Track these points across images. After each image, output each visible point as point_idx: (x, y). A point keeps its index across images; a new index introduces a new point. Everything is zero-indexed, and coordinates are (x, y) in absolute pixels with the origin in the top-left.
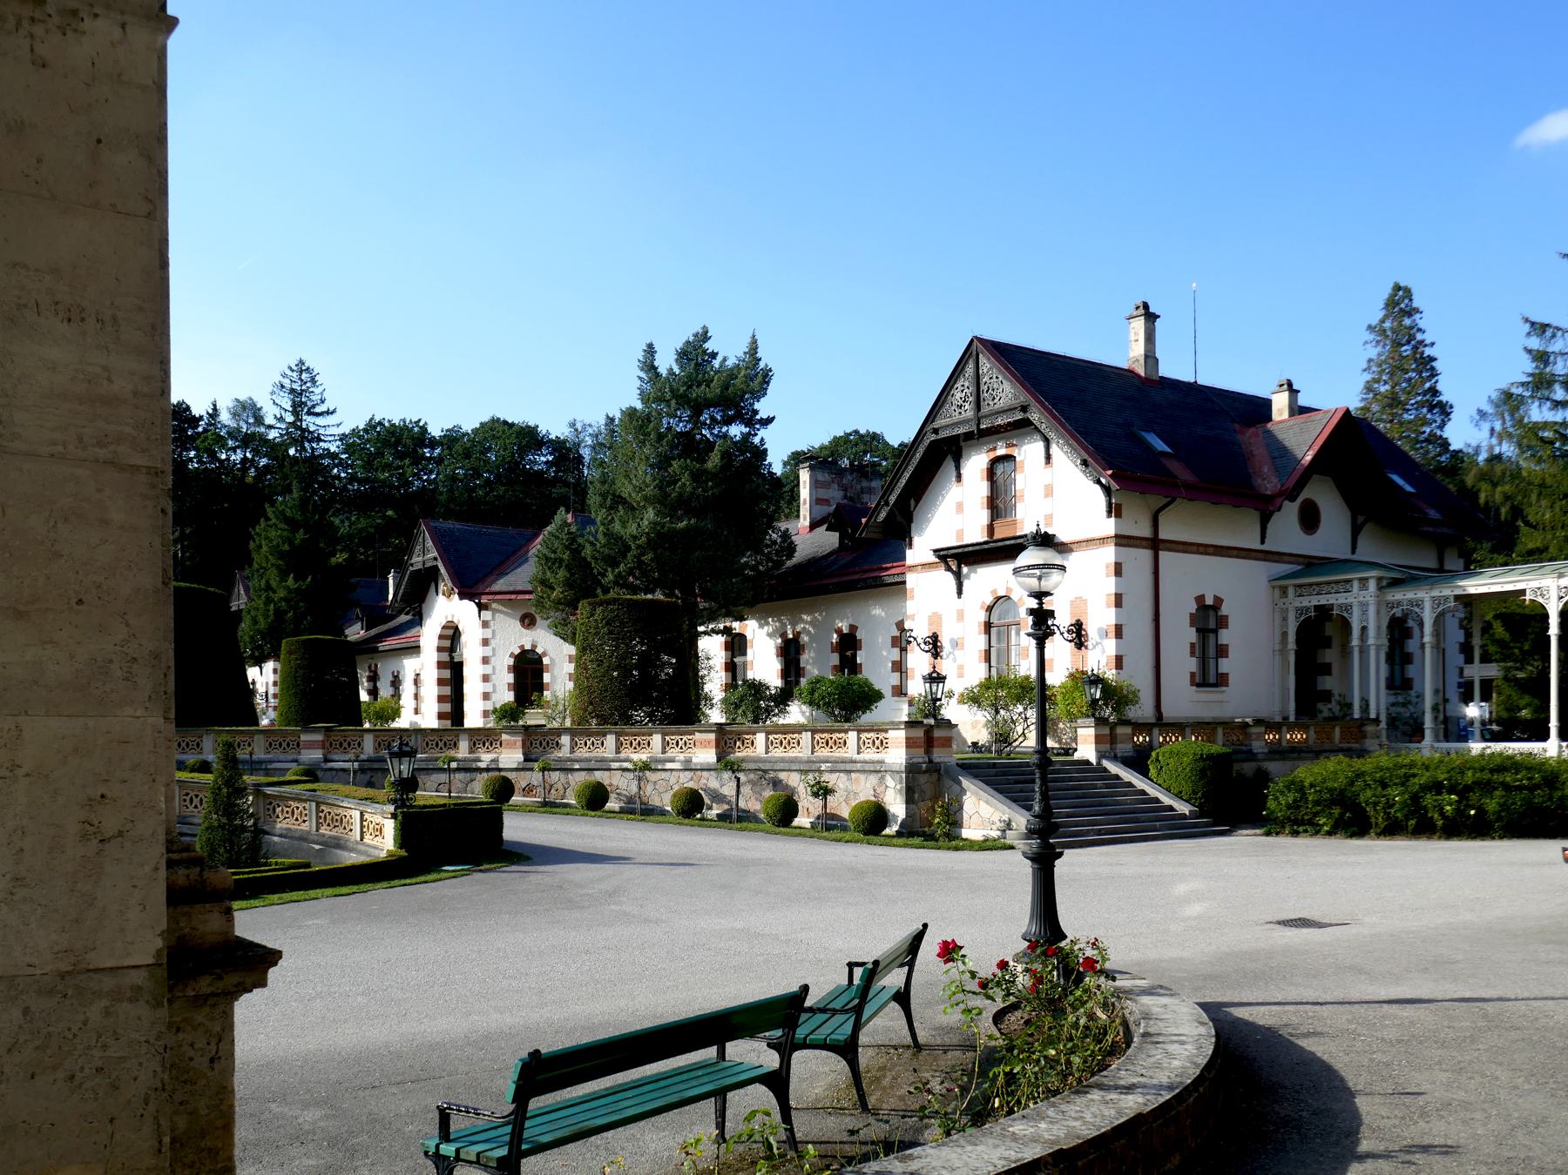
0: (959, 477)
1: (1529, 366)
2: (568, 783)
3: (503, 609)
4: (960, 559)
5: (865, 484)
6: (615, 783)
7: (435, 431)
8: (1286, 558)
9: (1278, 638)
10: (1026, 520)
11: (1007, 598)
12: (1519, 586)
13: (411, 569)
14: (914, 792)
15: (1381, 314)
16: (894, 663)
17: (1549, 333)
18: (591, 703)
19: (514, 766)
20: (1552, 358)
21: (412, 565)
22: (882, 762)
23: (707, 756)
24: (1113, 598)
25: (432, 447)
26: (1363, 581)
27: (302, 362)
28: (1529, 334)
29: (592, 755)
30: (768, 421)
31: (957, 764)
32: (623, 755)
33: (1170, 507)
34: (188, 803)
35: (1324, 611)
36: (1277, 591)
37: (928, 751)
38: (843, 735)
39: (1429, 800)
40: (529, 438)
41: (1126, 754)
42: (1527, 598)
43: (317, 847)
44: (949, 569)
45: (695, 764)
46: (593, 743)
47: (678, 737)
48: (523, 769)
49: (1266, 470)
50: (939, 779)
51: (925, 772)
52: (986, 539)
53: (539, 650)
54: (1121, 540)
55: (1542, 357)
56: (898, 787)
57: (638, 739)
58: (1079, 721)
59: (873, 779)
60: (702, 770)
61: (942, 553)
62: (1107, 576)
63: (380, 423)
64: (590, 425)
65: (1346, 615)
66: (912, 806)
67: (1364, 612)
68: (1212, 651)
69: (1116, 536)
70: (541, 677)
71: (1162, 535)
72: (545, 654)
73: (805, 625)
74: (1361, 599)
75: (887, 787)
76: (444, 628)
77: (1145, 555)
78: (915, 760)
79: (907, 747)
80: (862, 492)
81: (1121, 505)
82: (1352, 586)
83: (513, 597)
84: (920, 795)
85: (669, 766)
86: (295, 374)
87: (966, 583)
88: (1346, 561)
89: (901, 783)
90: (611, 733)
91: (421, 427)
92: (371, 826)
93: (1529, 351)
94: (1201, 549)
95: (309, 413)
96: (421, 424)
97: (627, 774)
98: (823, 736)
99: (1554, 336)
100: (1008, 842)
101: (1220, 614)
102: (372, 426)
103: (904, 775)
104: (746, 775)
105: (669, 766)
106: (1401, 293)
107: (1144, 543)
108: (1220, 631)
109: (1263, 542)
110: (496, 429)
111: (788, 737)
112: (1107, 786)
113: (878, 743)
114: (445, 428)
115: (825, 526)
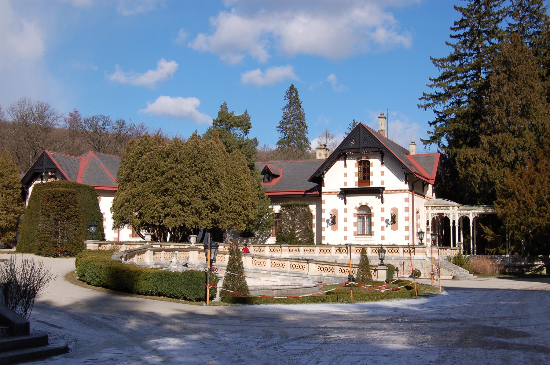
4: (345, 193)
10: (375, 182)
38: (397, 249)
62: (405, 202)
65: (448, 216)
67: (454, 216)
74: (453, 212)
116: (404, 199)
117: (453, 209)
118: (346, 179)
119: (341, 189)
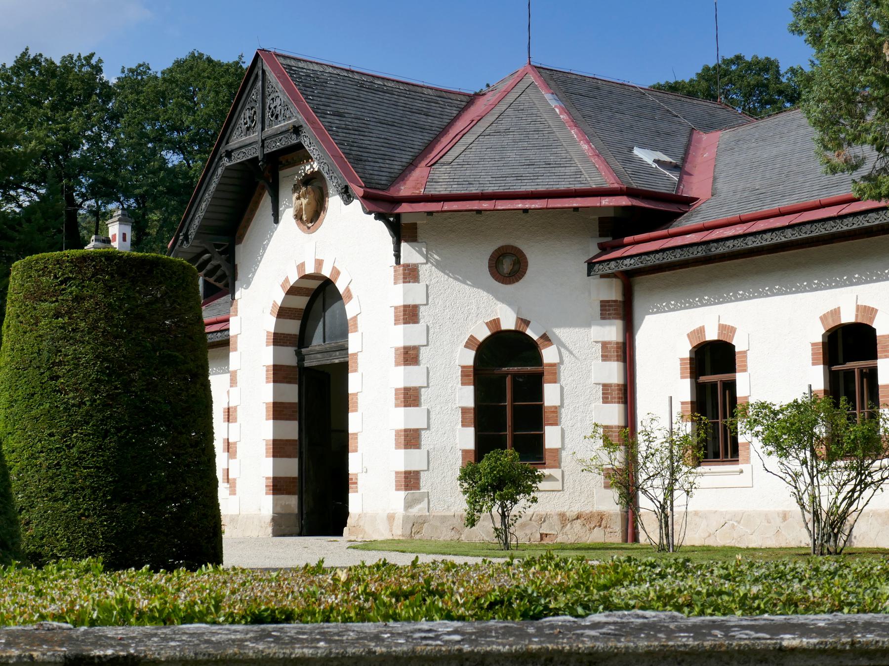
7: (111, 76)
13: (226, 162)
63: (36, 61)
76: (293, 291)
83: (485, 205)
91: (92, 67)
96: (93, 61)
102: (25, 64)
114: (127, 67)
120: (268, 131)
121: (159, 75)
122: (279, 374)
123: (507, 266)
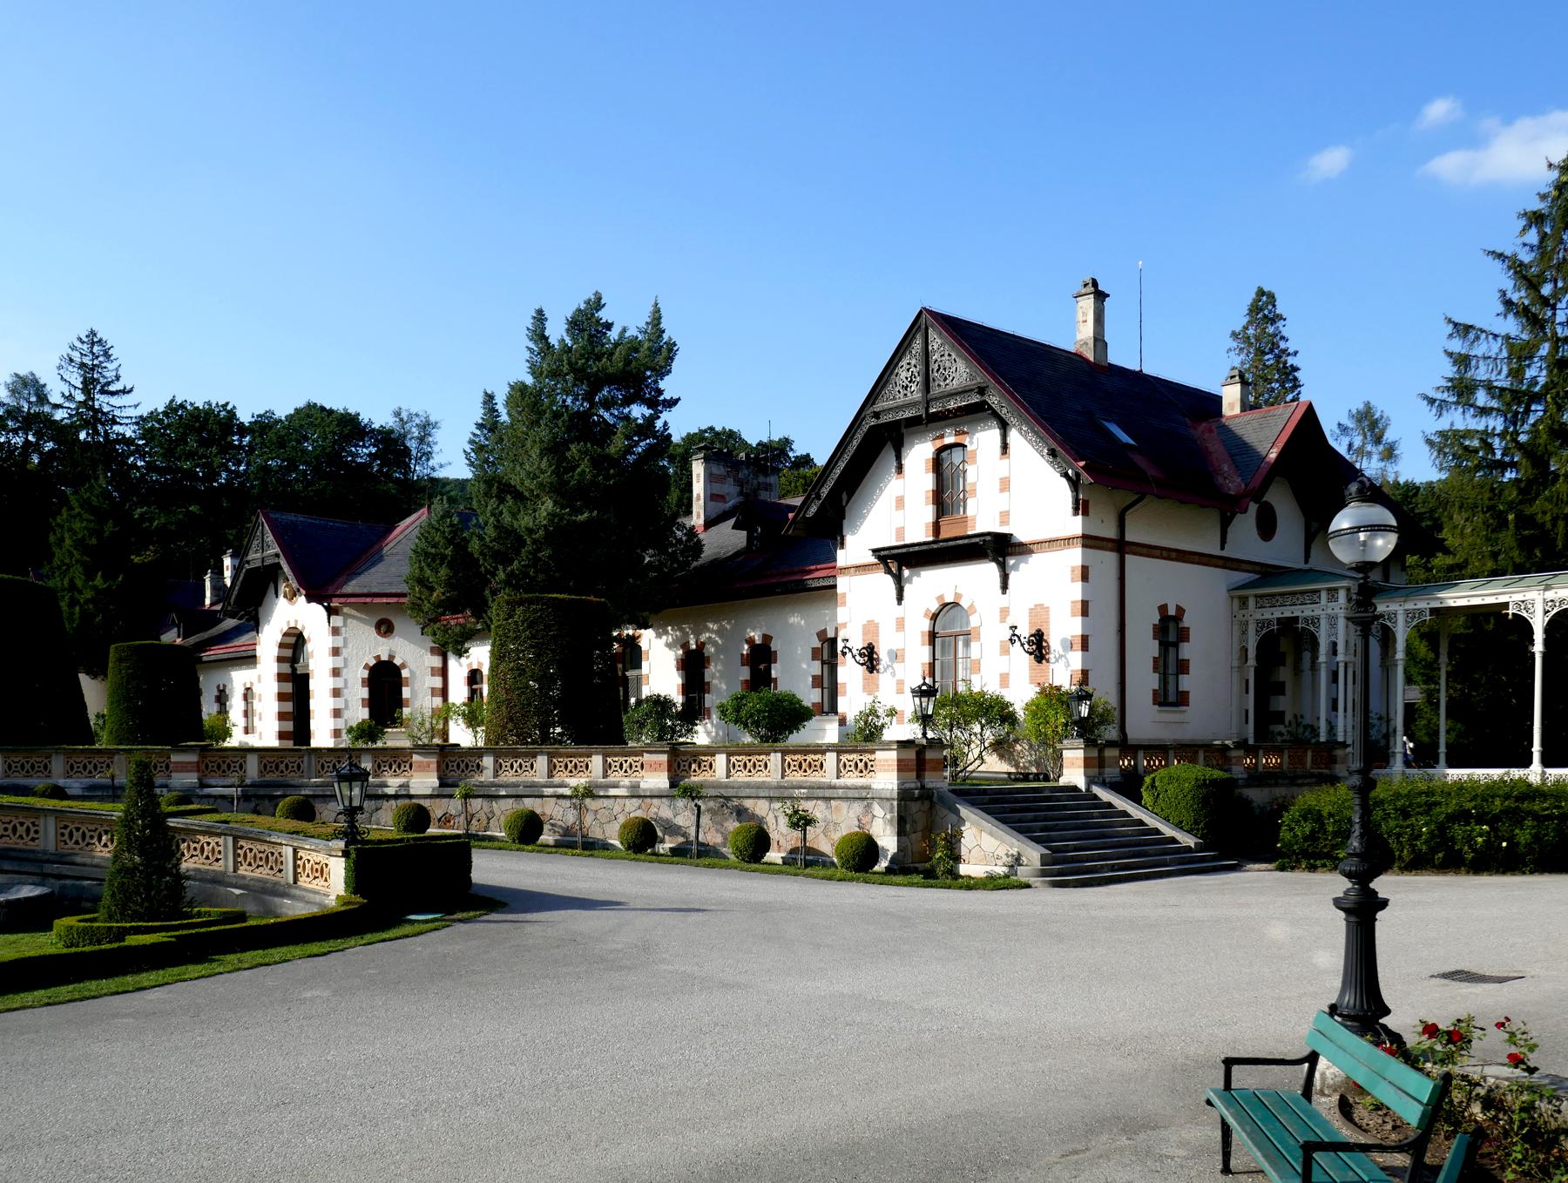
0: (900, 469)
1: (1450, 370)
2: (492, 812)
3: (358, 615)
5: (761, 479)
6: (548, 812)
7: (245, 417)
8: (1244, 566)
9: (1236, 654)
10: (982, 517)
11: (956, 604)
12: (1502, 599)
13: (247, 566)
14: (905, 822)
15: (1245, 320)
16: (814, 677)
17: (1472, 336)
18: (511, 719)
19: (429, 792)
20: (1473, 363)
21: (248, 562)
22: (868, 788)
23: (658, 780)
24: (1079, 606)
25: (242, 436)
26: (1332, 592)
27: (93, 333)
28: (1451, 335)
29: (519, 779)
30: (672, 403)
31: (953, 791)
32: (556, 780)
33: (1136, 507)
34: (66, 837)
35: (1288, 624)
36: (1236, 602)
37: (919, 777)
38: (819, 756)
39: (1458, 830)
40: (350, 427)
41: (1113, 780)
42: (1510, 612)
43: (237, 892)
44: (889, 571)
45: (644, 790)
46: (521, 766)
47: (622, 759)
48: (438, 796)
49: (1226, 469)
50: (931, 808)
51: (917, 799)
52: (931, 539)
53: (397, 662)
54: (1089, 541)
55: (1463, 361)
56: (888, 816)
57: (575, 760)
58: (1065, 742)
59: (857, 808)
60: (652, 797)
61: (882, 553)
62: (1073, 580)
63: (182, 406)
64: (417, 415)
66: (904, 839)
68: (1172, 668)
69: (1084, 537)
70: (400, 693)
71: (1129, 537)
72: (404, 666)
73: (711, 635)
74: (1330, 611)
75: (874, 816)
77: (1109, 558)
78: (907, 786)
79: (899, 770)
80: (759, 489)
81: (1087, 501)
82: (1319, 597)
83: (368, 600)
84: (912, 826)
85: (612, 792)
86: (85, 347)
87: (907, 588)
88: (1300, 570)
89: (891, 812)
90: (542, 753)
91: (228, 412)
92: (308, 866)
93: (1450, 355)
94: (1165, 554)
95: (103, 392)
96: (229, 408)
97: (562, 802)
98: (795, 757)
99: (1478, 338)
100: (1023, 880)
101: (1181, 625)
102: (172, 408)
103: (895, 803)
104: (704, 802)
105: (612, 792)
106: (1264, 298)
107: (1110, 545)
108: (1181, 644)
109: (1222, 548)
110: (312, 415)
111: (754, 759)
112: (1104, 816)
113: (861, 765)
115: (733, 521)
116: (1070, 569)
117: (1329, 600)
118: (898, 519)
119: (874, 551)
120: (266, 554)
121: (283, 418)
122: (281, 677)
123: (383, 629)
